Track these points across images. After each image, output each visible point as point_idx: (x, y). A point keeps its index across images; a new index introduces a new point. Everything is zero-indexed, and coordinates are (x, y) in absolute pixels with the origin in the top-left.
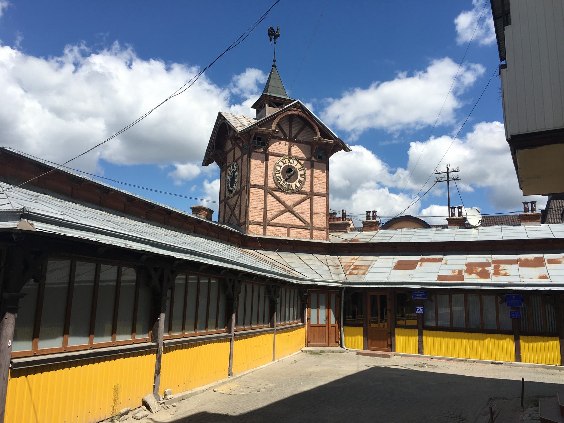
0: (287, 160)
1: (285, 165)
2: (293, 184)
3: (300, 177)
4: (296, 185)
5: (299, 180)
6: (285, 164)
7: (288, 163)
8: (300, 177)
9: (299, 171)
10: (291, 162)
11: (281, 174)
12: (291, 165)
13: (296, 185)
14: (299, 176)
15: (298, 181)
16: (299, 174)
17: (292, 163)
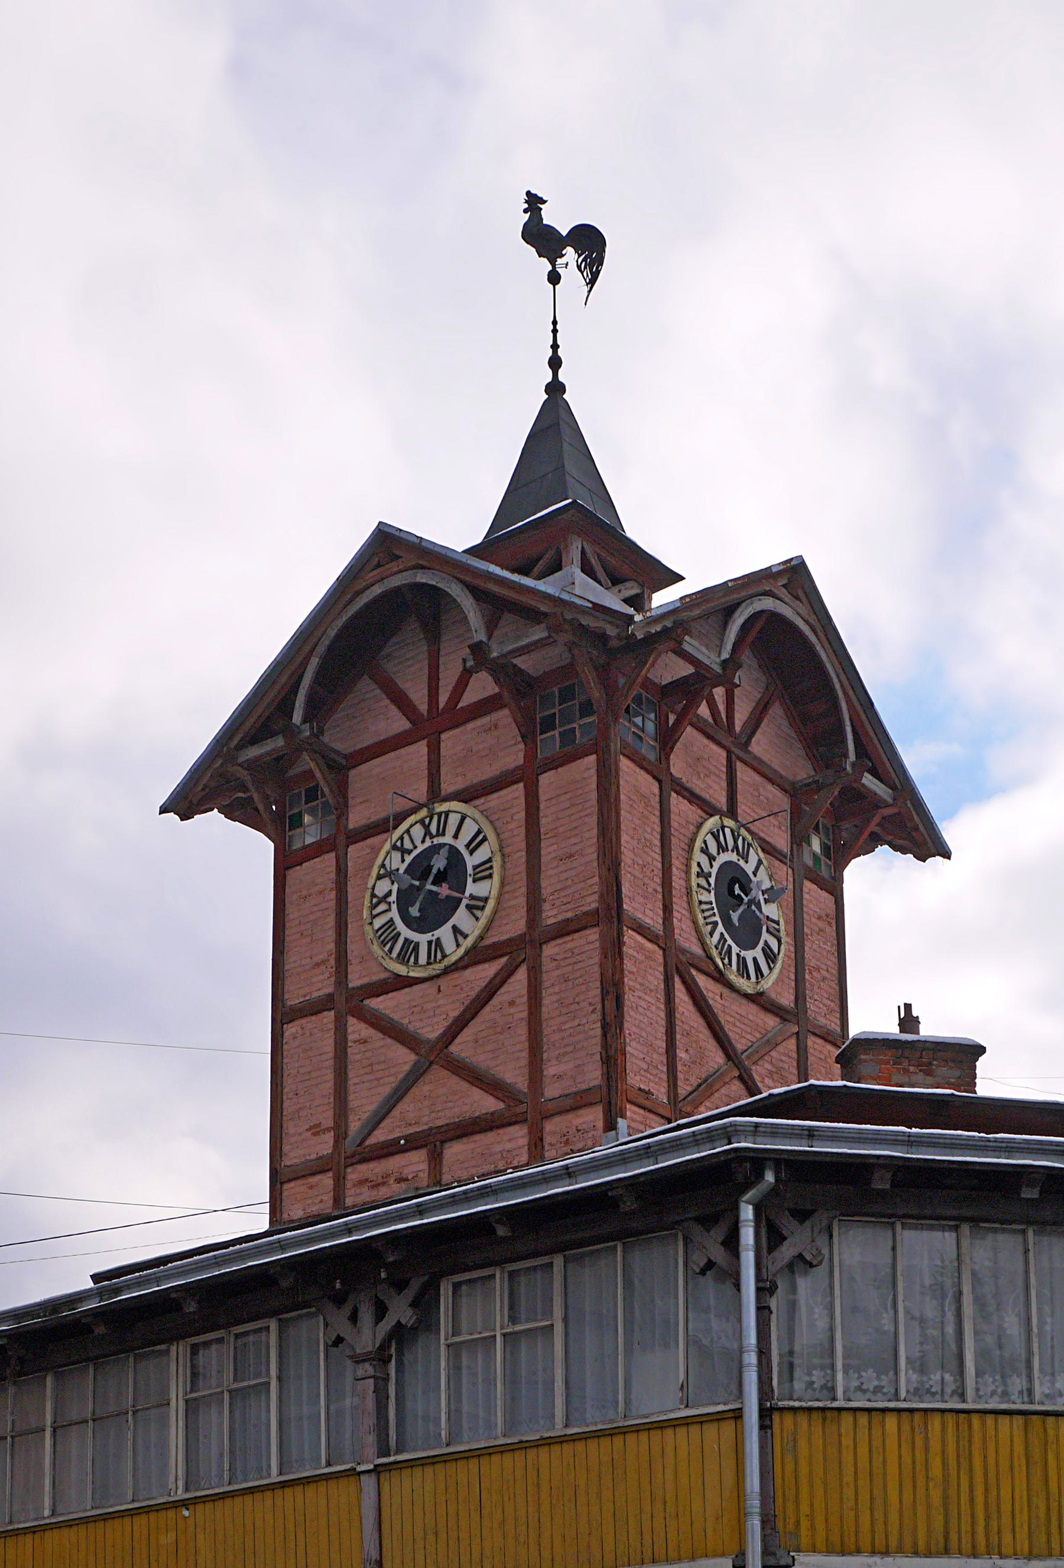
0: (418, 832)
1: (409, 859)
2: (444, 933)
3: (474, 881)
4: (456, 929)
5: (472, 897)
6: (410, 852)
7: (423, 842)
8: (474, 881)
9: (471, 853)
10: (433, 829)
11: (394, 907)
12: (436, 841)
13: (456, 929)
14: (470, 880)
15: (468, 906)
16: (470, 870)
17: (438, 835)
